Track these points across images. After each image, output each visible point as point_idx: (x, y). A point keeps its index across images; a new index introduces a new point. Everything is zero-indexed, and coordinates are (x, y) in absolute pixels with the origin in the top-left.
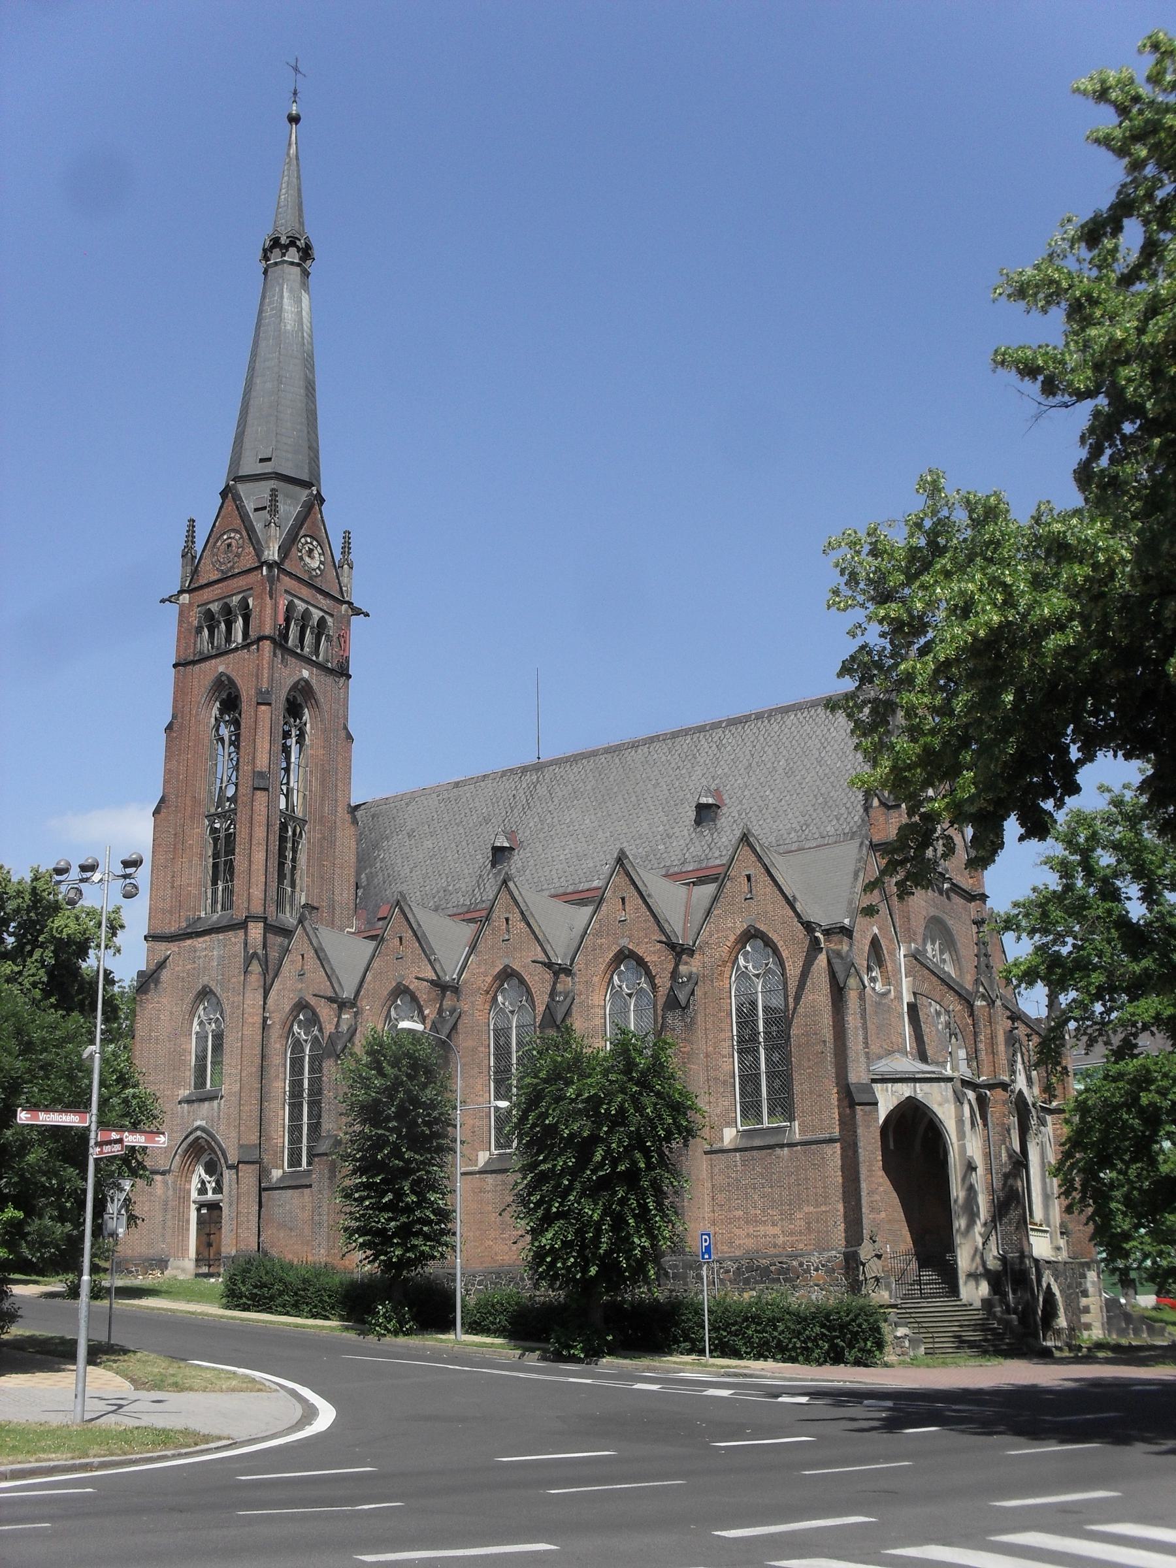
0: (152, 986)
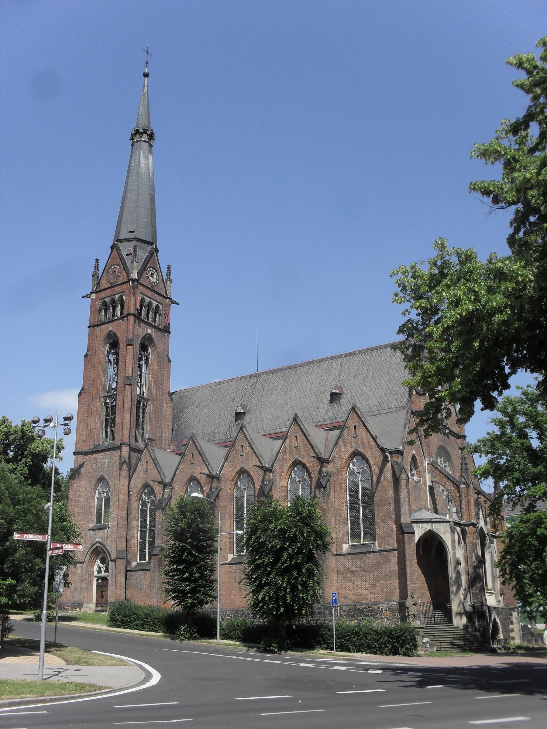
0: (77, 476)
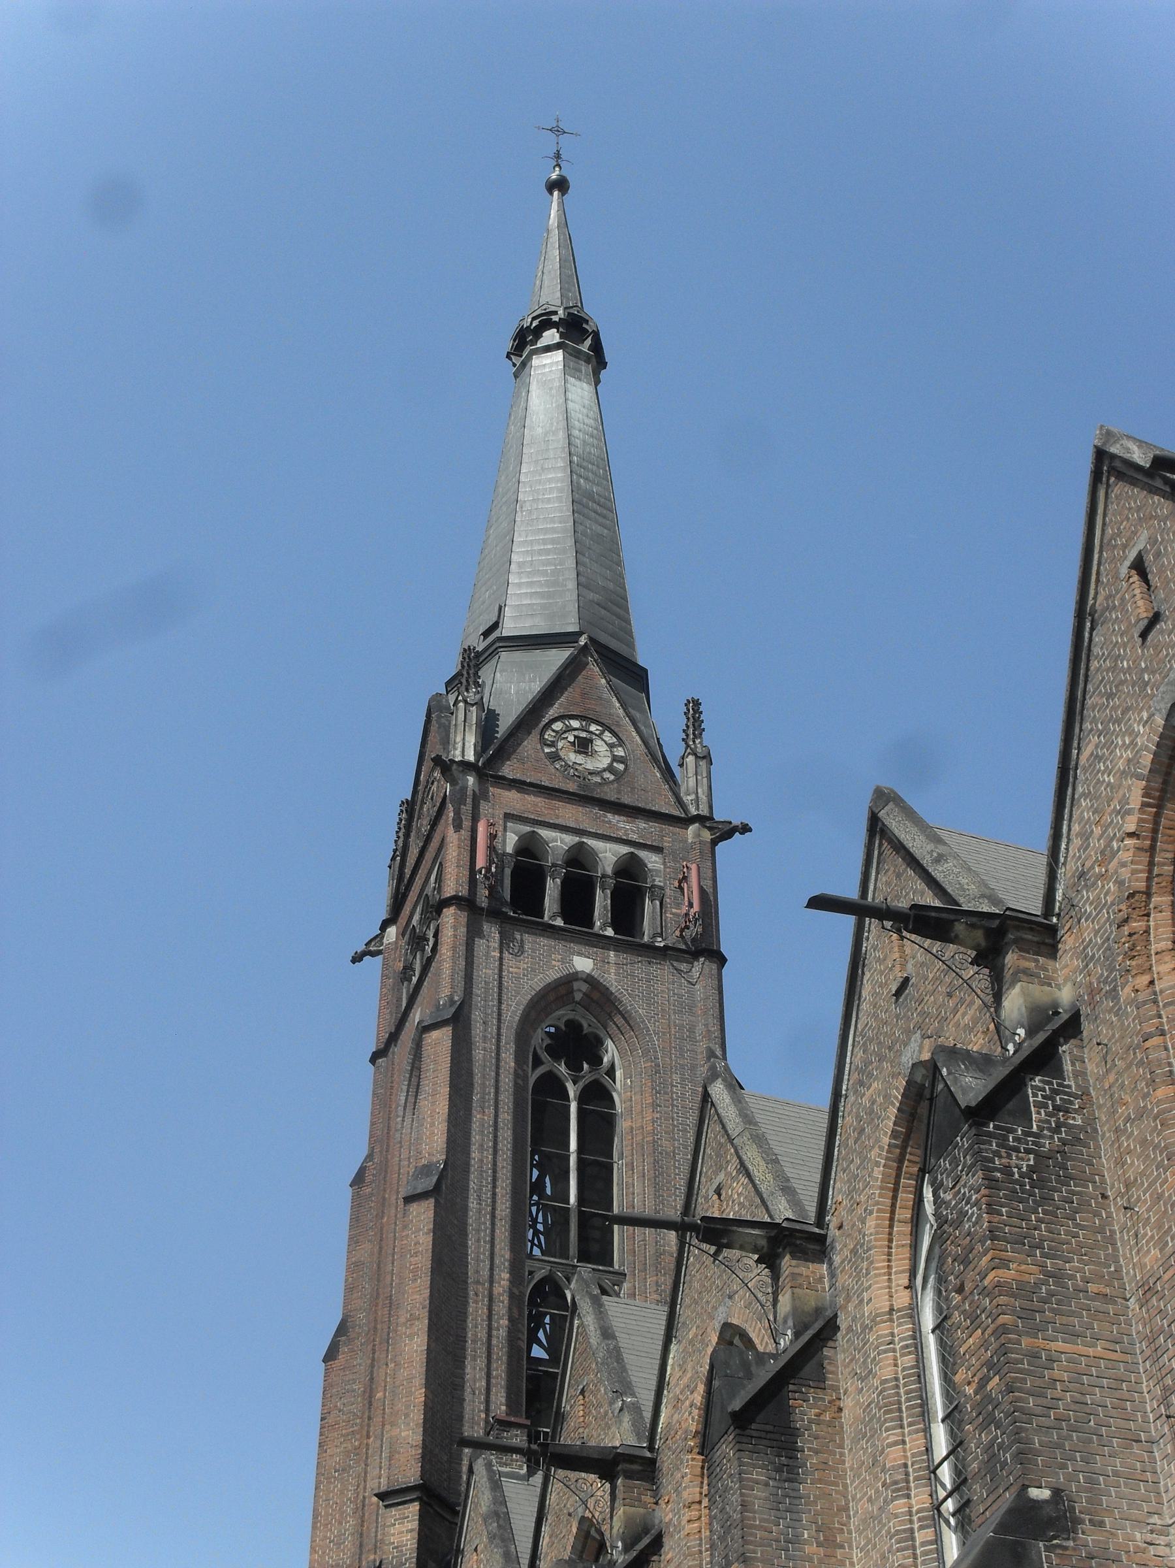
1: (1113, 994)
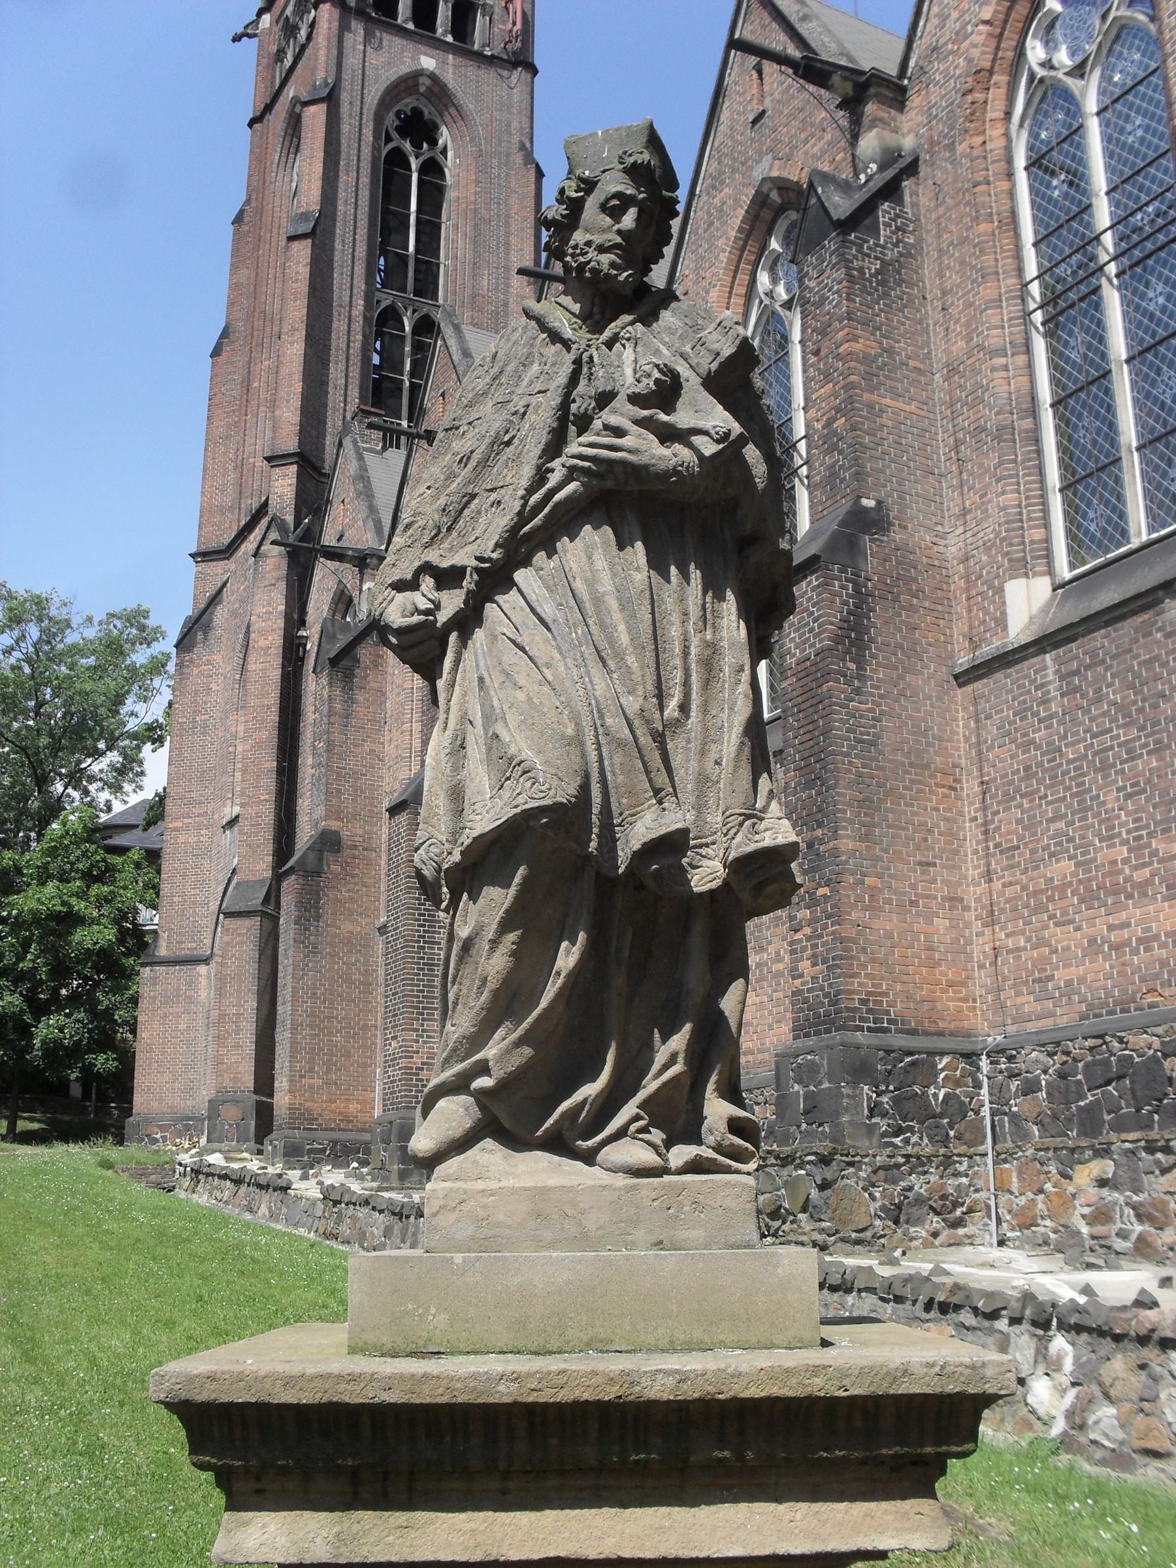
0: (200, 636)
1: (951, 147)
